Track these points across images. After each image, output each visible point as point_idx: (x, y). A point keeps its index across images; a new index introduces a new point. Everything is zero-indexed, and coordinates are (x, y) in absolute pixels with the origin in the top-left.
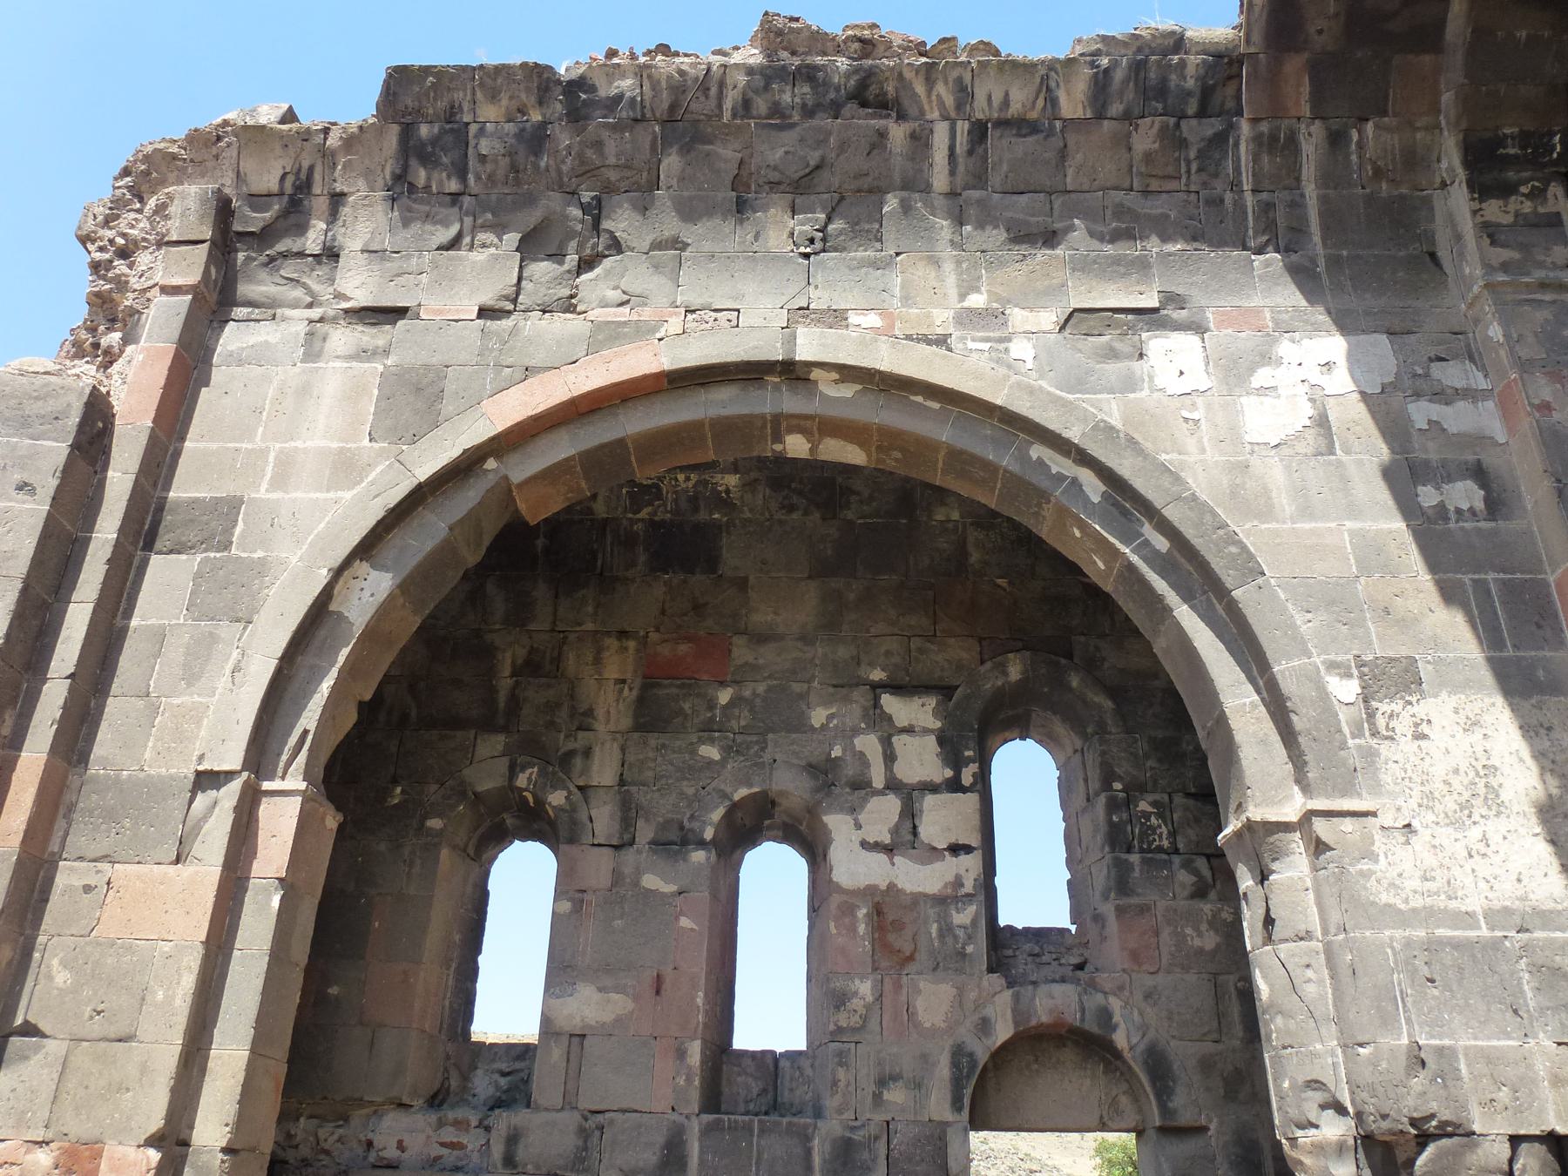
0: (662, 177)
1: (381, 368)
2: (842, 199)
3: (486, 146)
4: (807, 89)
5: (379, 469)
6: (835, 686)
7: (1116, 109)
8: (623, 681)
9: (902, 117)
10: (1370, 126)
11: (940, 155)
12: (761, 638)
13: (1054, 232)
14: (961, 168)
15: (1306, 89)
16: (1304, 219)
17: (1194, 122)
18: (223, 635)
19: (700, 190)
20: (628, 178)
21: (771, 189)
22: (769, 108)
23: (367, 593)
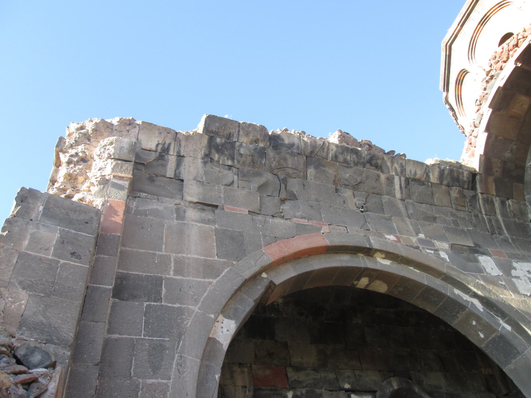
0: (308, 175)
1: (213, 227)
2: (368, 195)
3: (243, 151)
4: (354, 156)
5: (226, 270)
6: (330, 391)
7: (445, 182)
8: (245, 387)
9: (382, 172)
10: (510, 201)
11: (397, 187)
12: (298, 369)
13: (436, 217)
14: (404, 192)
15: (494, 187)
16: (500, 225)
17: (466, 191)
18: (167, 346)
19: (322, 182)
20: (295, 173)
21: (345, 187)
22: (343, 160)
23: (225, 330)
